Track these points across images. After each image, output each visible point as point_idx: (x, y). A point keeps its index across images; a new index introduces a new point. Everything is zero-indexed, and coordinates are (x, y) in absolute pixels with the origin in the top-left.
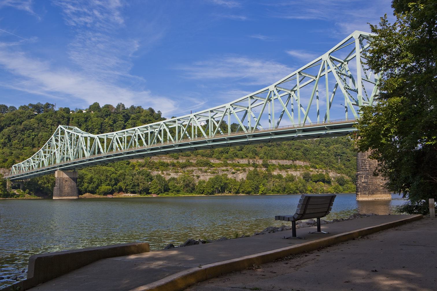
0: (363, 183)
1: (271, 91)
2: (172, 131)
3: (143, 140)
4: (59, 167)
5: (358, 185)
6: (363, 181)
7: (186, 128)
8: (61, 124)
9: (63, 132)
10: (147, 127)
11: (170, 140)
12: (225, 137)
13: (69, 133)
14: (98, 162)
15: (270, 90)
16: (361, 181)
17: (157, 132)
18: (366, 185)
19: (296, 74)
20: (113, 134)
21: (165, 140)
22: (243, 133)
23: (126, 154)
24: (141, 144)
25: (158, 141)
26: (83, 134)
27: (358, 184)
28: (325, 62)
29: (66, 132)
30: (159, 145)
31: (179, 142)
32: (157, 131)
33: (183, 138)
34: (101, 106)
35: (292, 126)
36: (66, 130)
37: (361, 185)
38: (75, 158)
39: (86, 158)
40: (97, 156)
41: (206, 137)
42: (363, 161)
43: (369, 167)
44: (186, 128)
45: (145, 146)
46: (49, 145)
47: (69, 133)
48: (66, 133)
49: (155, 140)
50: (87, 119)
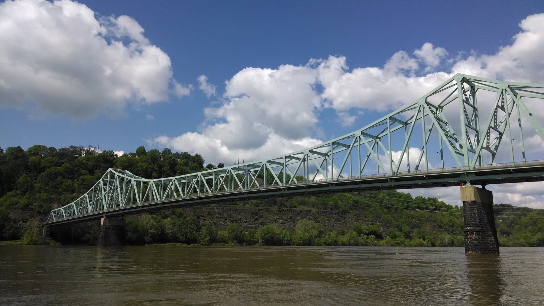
0: (474, 240)
1: (357, 137)
2: (209, 182)
3: (180, 190)
4: (106, 213)
5: (469, 242)
6: (474, 238)
7: (223, 179)
8: (111, 167)
9: (113, 176)
10: (184, 177)
11: (207, 191)
12: (357, 181)
13: (120, 176)
14: (175, 206)
15: (356, 136)
16: (472, 238)
17: (194, 183)
18: (477, 242)
19: (387, 119)
20: (172, 179)
21: (202, 191)
22: (278, 186)
23: (186, 201)
24: (179, 195)
25: (195, 191)
26: (134, 179)
27: (468, 241)
28: (422, 106)
29: (116, 175)
30: (196, 196)
31: (187, 197)
32: (195, 181)
33: (220, 189)
34: (147, 150)
35: (365, 176)
36: (117, 174)
37: (472, 243)
38: (126, 204)
39: (121, 207)
40: (131, 205)
41: (281, 185)
42: (472, 215)
43: (480, 222)
44: (223, 179)
45: (183, 197)
46: (95, 189)
47: (119, 177)
48: (117, 177)
49: (191, 191)
50: (91, 172)
